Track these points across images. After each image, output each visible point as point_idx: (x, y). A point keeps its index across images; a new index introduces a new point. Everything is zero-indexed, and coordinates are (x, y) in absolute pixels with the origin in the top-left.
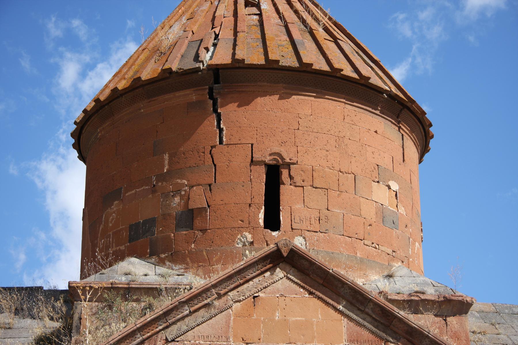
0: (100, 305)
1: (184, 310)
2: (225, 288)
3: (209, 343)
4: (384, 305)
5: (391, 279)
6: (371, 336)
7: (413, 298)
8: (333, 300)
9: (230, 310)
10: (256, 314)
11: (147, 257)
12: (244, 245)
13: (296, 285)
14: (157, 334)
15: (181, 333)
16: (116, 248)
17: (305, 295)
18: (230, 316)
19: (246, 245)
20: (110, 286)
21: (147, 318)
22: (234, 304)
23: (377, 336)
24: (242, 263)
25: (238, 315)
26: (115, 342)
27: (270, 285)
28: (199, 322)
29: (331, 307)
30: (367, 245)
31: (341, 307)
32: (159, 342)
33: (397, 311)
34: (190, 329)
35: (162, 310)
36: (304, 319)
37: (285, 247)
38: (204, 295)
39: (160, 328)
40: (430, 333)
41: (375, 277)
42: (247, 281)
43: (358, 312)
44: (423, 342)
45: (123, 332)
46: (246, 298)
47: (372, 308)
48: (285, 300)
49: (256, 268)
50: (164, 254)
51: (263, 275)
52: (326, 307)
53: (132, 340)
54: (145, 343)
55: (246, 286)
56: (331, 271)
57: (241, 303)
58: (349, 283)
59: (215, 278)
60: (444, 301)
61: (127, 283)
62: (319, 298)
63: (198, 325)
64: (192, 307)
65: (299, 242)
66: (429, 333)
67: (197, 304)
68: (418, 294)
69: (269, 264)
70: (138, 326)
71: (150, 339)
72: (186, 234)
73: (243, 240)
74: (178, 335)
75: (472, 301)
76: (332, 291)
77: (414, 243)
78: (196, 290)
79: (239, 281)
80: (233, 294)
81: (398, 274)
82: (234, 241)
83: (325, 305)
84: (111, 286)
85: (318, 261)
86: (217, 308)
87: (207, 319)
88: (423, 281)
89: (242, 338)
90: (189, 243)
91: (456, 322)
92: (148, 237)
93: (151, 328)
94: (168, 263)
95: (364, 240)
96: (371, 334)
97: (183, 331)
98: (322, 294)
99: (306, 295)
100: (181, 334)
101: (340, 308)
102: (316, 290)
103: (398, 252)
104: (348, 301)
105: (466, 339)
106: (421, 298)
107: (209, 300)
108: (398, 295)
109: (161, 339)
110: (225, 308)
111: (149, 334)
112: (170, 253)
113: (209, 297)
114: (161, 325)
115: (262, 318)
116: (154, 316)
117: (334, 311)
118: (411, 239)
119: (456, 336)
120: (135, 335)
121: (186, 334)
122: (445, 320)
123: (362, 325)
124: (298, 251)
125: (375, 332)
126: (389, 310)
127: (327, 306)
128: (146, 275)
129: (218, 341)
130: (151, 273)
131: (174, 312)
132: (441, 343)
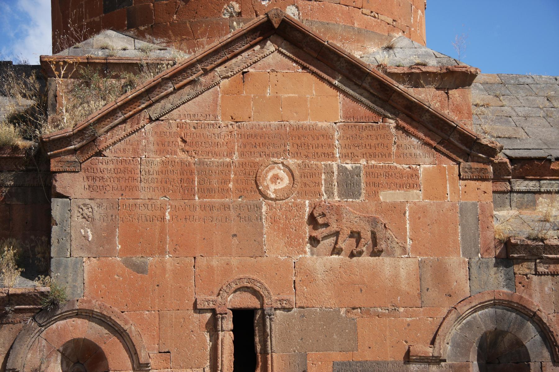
0: (77, 82)
1: (167, 87)
2: (212, 63)
3: (196, 121)
4: (382, 79)
5: (391, 51)
6: (368, 112)
7: (413, 71)
8: (328, 75)
9: (217, 87)
10: (246, 91)
11: (124, 29)
12: (232, 16)
13: (288, 59)
15: (166, 111)
16: (89, 20)
17: (298, 70)
18: (217, 93)
19: (233, 16)
20: (86, 61)
21: (128, 96)
22: (221, 81)
23: (374, 111)
24: (230, 36)
25: (226, 92)
26: (95, 121)
27: (260, 59)
28: (185, 100)
29: (326, 82)
30: (365, 14)
31: (337, 82)
32: (142, 121)
33: (397, 85)
34: (175, 107)
35: (144, 87)
36: (297, 95)
37: (276, 18)
38: (189, 71)
39: (143, 106)
40: (430, 107)
41: (373, 49)
42: (236, 56)
43: (355, 87)
44: (423, 117)
45: (103, 111)
46: (234, 74)
47: (369, 83)
48: (276, 76)
49: (244, 41)
50: (144, 27)
51: (252, 49)
52: (321, 83)
53: (113, 119)
55: (234, 61)
56: (326, 43)
57: (230, 79)
58: (346, 56)
59: (200, 53)
60: (447, 72)
61: (104, 58)
62: (313, 73)
63: (184, 103)
64: (177, 83)
65: (291, 12)
66: (429, 107)
67: (181, 81)
68: (419, 67)
69: (259, 37)
70: (118, 104)
72: (166, 4)
73: (230, 10)
74: (162, 114)
76: (327, 65)
77: (417, 10)
78: (180, 65)
79: (227, 55)
80: (220, 70)
81: (398, 45)
82: (220, 12)
83: (320, 80)
84: (87, 61)
85: (312, 33)
86: (204, 85)
87: (193, 97)
88: (425, 52)
89: (231, 117)
90: (170, 14)
92: (125, 7)
93: (133, 106)
94: (148, 36)
95: (362, 8)
96: (368, 110)
97: (167, 109)
98: (317, 68)
99: (300, 70)
100: (165, 113)
101: (335, 84)
102: (310, 64)
103: (399, 21)
104: (344, 75)
105: (468, 112)
106: (422, 70)
107: (194, 77)
108: (398, 68)
109: (144, 118)
110: (212, 85)
111: (131, 113)
112: (150, 25)
113: (195, 74)
114: (143, 103)
115: (252, 96)
116: (136, 93)
117: (329, 86)
118: (413, 7)
120: (116, 114)
121: (171, 112)
122: (447, 93)
123: (359, 100)
124: (291, 22)
125: (372, 107)
126: (388, 84)
127: (322, 81)
128: (124, 49)
129: (205, 120)
130: (130, 47)
131: (158, 89)
132: (442, 116)
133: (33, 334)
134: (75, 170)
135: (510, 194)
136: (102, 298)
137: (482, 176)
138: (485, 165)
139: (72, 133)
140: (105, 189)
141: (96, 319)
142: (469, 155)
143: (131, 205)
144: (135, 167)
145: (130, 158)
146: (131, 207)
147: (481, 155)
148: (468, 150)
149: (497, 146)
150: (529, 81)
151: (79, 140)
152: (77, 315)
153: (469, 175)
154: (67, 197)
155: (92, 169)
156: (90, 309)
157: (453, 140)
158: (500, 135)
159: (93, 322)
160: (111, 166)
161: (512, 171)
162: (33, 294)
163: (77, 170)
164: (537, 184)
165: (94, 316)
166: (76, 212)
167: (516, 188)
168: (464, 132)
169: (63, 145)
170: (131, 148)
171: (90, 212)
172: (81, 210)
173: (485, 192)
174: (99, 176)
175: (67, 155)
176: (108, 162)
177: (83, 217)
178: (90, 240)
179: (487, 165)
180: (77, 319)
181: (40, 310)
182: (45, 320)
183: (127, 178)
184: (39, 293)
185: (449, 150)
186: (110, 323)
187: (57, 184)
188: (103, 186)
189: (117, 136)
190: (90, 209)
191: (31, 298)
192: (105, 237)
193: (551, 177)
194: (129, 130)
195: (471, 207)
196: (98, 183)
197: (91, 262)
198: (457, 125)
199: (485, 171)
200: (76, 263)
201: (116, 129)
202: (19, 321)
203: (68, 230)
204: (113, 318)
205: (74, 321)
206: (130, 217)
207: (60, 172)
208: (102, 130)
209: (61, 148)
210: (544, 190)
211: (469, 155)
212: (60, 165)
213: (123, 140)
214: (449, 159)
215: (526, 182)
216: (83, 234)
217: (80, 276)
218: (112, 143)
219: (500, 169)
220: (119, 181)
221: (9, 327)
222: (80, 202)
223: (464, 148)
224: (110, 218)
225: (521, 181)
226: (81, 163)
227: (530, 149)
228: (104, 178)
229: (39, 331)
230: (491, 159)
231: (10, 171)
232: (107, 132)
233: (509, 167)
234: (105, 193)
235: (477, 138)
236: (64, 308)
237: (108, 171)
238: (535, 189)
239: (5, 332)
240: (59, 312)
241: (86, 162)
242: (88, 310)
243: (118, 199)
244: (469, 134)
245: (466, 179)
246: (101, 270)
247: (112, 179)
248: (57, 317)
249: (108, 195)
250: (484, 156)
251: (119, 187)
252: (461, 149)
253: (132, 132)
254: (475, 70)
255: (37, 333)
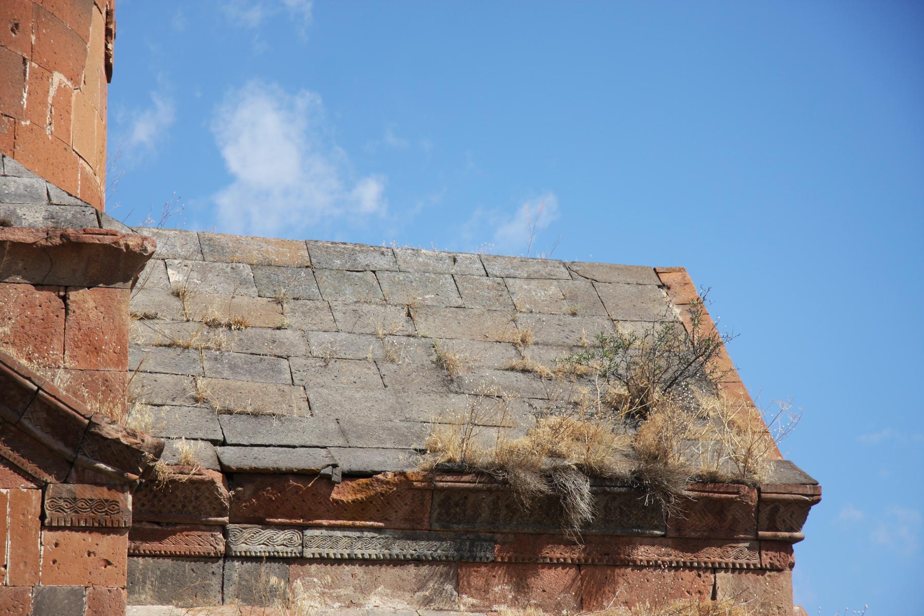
60: (62, 245)
75: (142, 247)
77: (47, 74)
88: (26, 187)
91: (94, 305)
105: (117, 350)
118: (32, 66)
119: (89, 343)
122: (64, 299)
135: (224, 562)
137: (102, 520)
138: (113, 492)
142: (71, 464)
147: (102, 466)
148: (68, 452)
149: (145, 444)
150: (382, 262)
153: (68, 516)
157: (30, 426)
158: (232, 407)
161: (231, 503)
164: (295, 538)
167: (240, 548)
168: (56, 406)
173: (108, 563)
179: (117, 491)
185: (18, 453)
193: (333, 522)
195: (66, 601)
198: (39, 388)
199: (111, 507)
210: (313, 554)
211: (71, 464)
214: (19, 474)
215: (268, 533)
219: (197, 498)
223: (58, 446)
225: (254, 530)
227: (294, 447)
230: (127, 478)
233: (221, 494)
235: (90, 422)
238: (289, 550)
244: (70, 411)
245: (58, 528)
250: (109, 469)
252: (51, 450)
254: (139, 241)
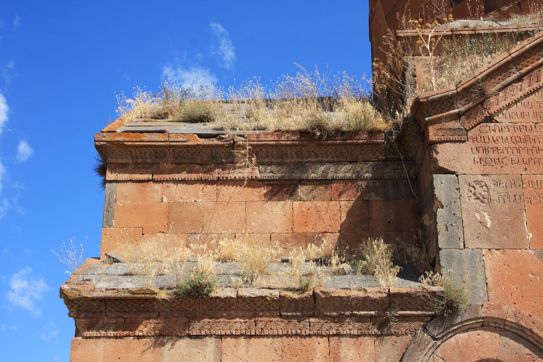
14: (540, 68)
20: (450, 33)
21: (524, 45)
26: (484, 77)
45: (494, 64)
50: (507, 6)
54: (523, 80)
61: (471, 29)
70: (513, 55)
71: (530, 75)
84: (451, 33)
93: (530, 60)
111: (528, 68)
112: (516, 3)
116: (535, 42)
120: (509, 69)
133: (427, 350)
134: (460, 139)
136: (515, 304)
139: (456, 91)
140: (502, 162)
141: (511, 333)
143: (539, 182)
144: (539, 135)
145: (531, 124)
146: (539, 185)
151: (463, 102)
152: (482, 326)
154: (453, 173)
155: (482, 138)
156: (501, 317)
159: (506, 336)
160: (506, 134)
162: (421, 294)
163: (463, 139)
165: (507, 328)
166: (467, 191)
169: (444, 109)
170: (531, 111)
171: (485, 191)
172: (472, 189)
174: (492, 147)
175: (448, 121)
176: (502, 129)
177: (476, 197)
178: (488, 226)
180: (483, 331)
181: (431, 318)
182: (442, 330)
183: (530, 148)
184: (429, 293)
186: (531, 339)
187: (438, 157)
188: (498, 159)
189: (511, 97)
190: (484, 187)
191: (418, 301)
192: (508, 223)
194: (527, 89)
196: (491, 155)
197: (493, 255)
200: (473, 256)
201: (509, 88)
202: (405, 332)
203: (458, 214)
204: (535, 330)
205: (479, 335)
206: (540, 197)
207: (441, 142)
208: (493, 90)
209: (442, 112)
212: (441, 133)
213: (519, 102)
216: (479, 218)
217: (480, 273)
218: (506, 105)
220: (519, 151)
221: (391, 340)
222: (471, 179)
224: (512, 198)
226: (467, 131)
228: (499, 148)
229: (433, 346)
231: (365, 161)
232: (500, 90)
234: (502, 167)
236: (464, 316)
237: (504, 140)
239: (387, 346)
240: (459, 320)
241: (473, 130)
242: (498, 318)
243: (521, 175)
246: (508, 266)
247: (510, 150)
248: (457, 327)
249: (507, 170)
251: (521, 160)
253: (530, 91)
255: (430, 348)
